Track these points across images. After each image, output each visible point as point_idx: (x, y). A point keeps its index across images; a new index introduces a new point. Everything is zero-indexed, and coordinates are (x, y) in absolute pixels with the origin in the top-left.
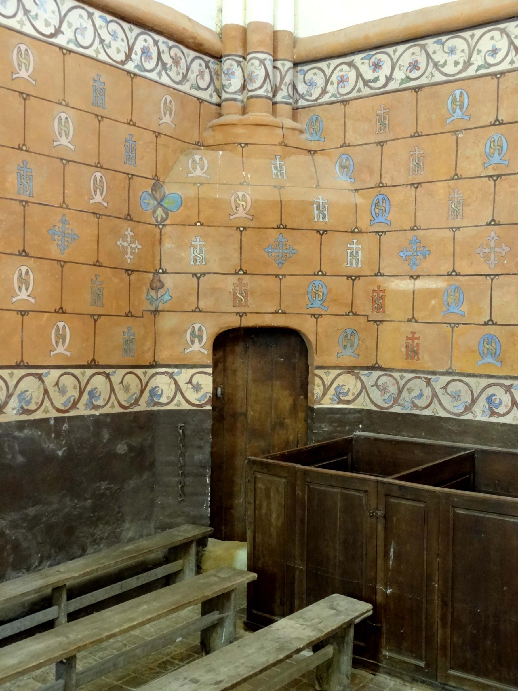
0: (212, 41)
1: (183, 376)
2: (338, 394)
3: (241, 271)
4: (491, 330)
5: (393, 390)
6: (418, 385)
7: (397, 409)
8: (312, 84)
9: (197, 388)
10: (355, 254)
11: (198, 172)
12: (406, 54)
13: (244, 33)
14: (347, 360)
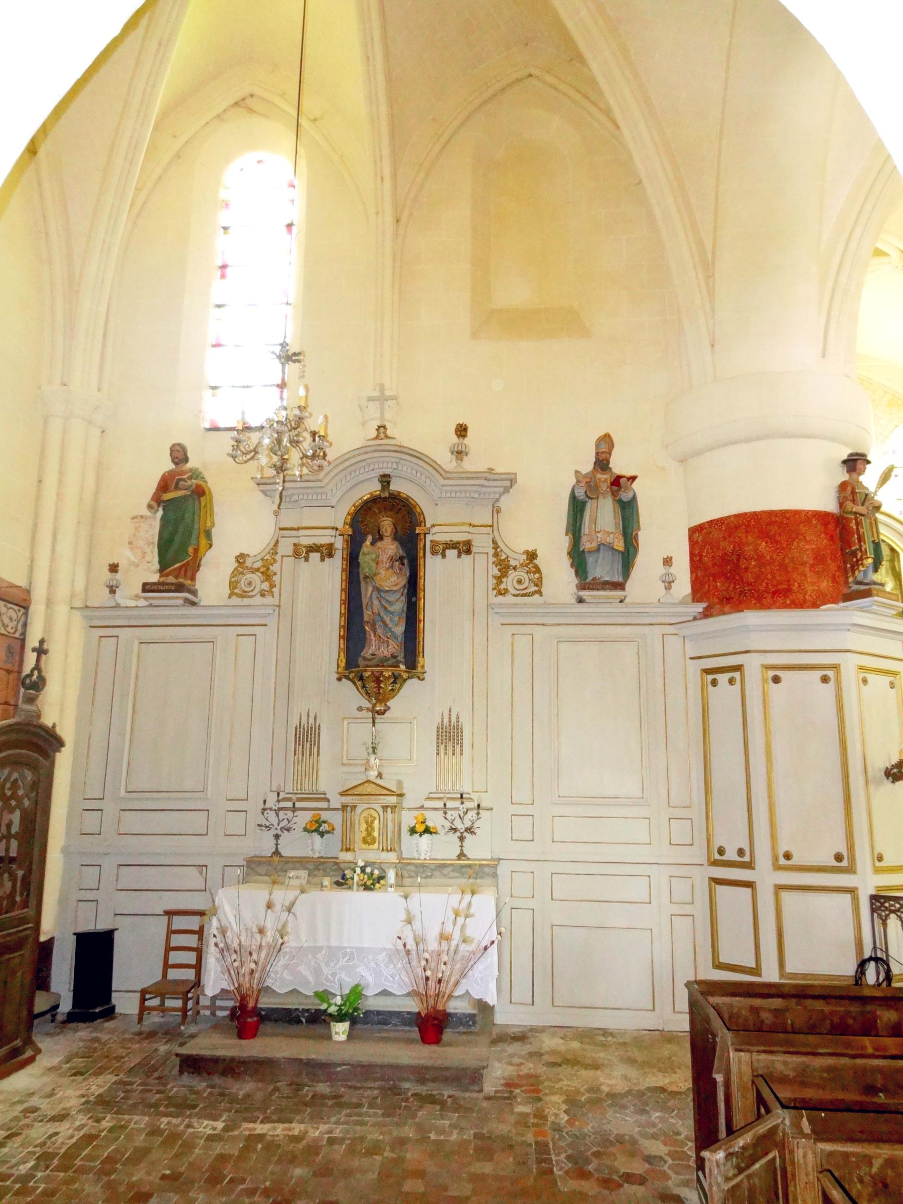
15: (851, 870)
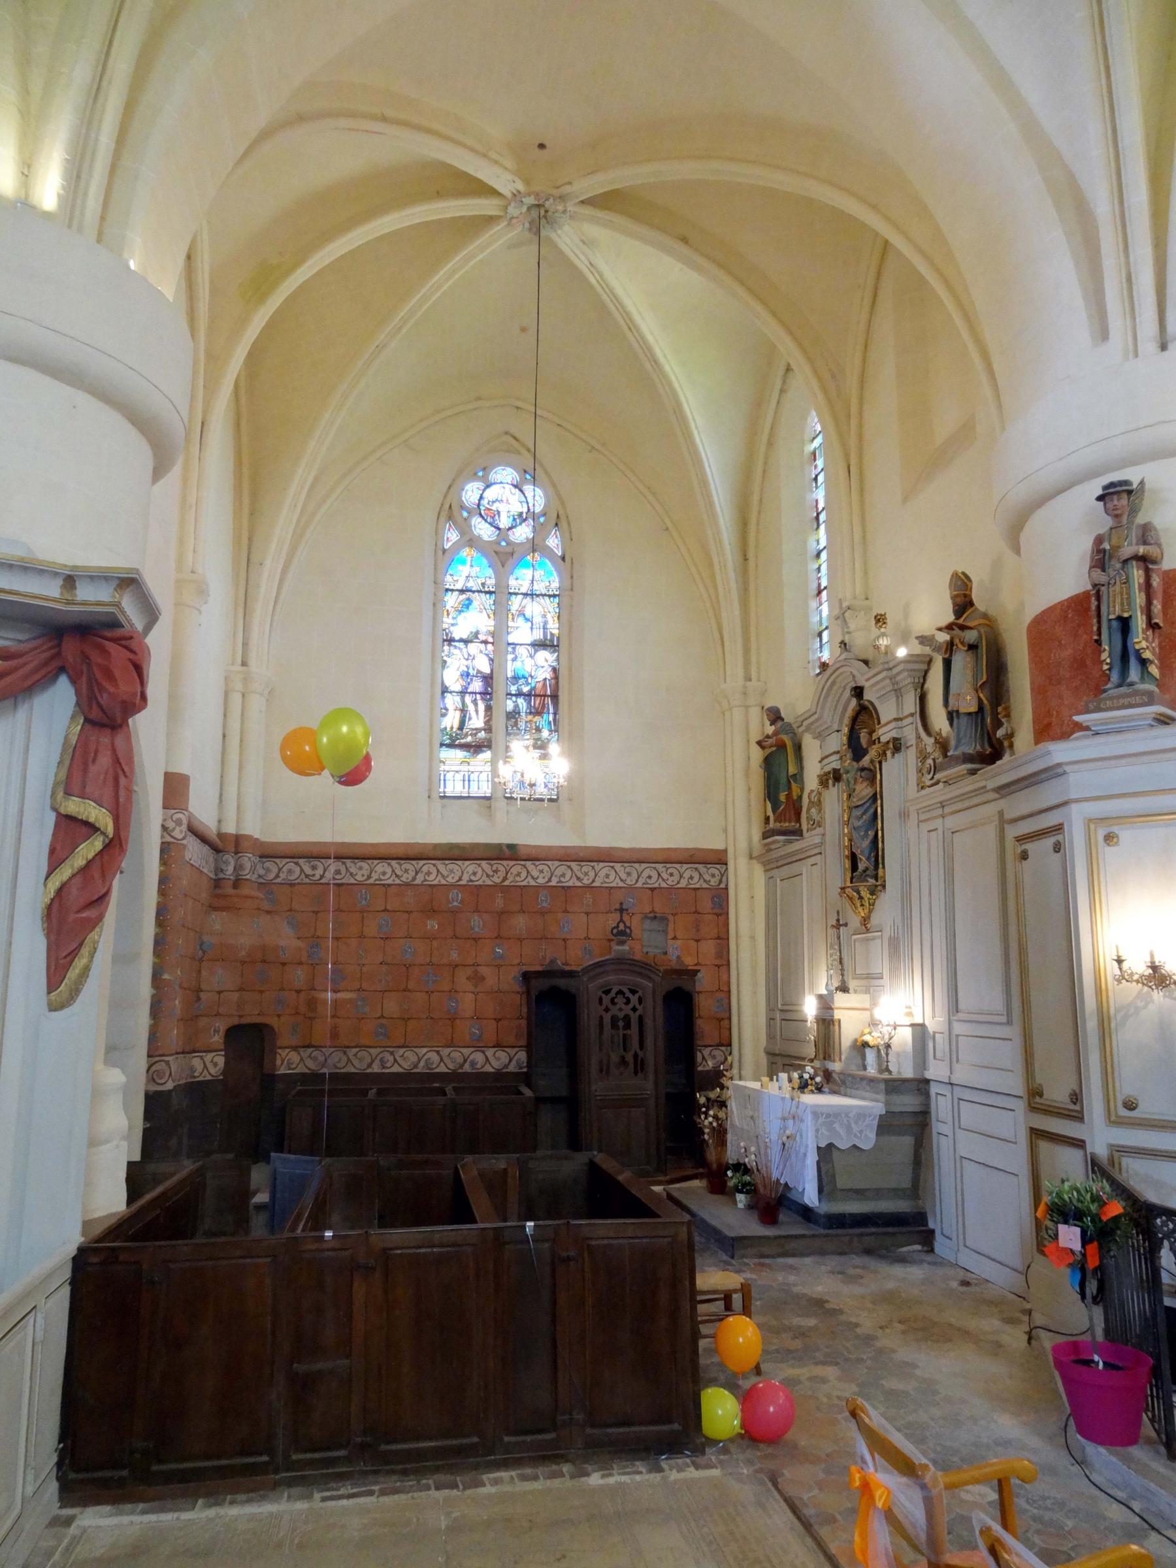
2: (289, 1063)
3: (241, 989)
4: (381, 1021)
5: (322, 1059)
8: (268, 870)
9: (216, 1065)
10: (299, 976)
11: (218, 927)
12: (333, 866)
14: (293, 1043)
15: (1078, 1117)
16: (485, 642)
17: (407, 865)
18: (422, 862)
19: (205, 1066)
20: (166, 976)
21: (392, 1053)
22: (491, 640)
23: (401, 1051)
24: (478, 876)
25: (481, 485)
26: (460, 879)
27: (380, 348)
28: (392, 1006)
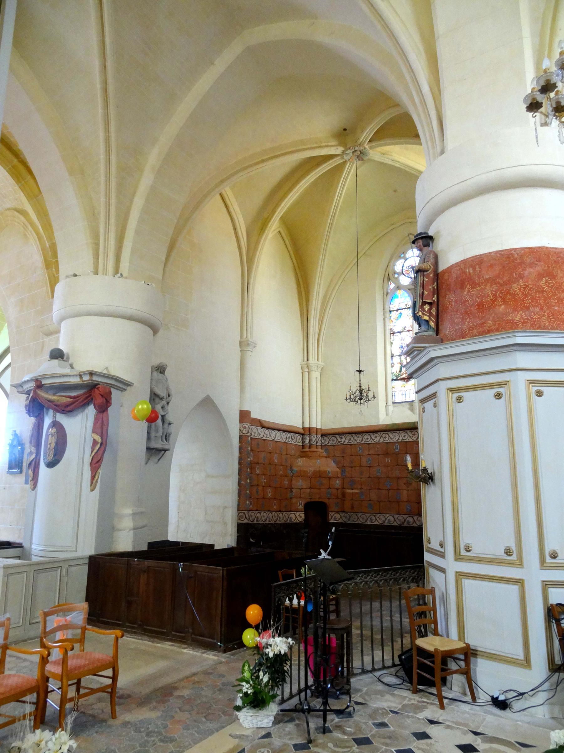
0: (302, 431)
1: (297, 514)
3: (310, 488)
4: (370, 502)
6: (354, 515)
7: (349, 522)
9: (301, 517)
11: (300, 464)
12: (349, 437)
13: (310, 429)
14: (336, 510)
16: (409, 331)
17: (376, 435)
18: (382, 433)
19: (296, 517)
20: (242, 482)
21: (375, 516)
22: (411, 329)
23: (379, 515)
24: (406, 437)
25: (403, 260)
26: (399, 439)
27: (331, 225)
28: (374, 495)
